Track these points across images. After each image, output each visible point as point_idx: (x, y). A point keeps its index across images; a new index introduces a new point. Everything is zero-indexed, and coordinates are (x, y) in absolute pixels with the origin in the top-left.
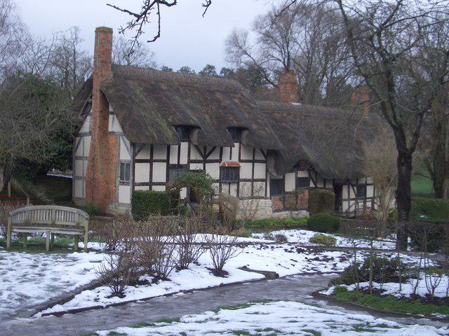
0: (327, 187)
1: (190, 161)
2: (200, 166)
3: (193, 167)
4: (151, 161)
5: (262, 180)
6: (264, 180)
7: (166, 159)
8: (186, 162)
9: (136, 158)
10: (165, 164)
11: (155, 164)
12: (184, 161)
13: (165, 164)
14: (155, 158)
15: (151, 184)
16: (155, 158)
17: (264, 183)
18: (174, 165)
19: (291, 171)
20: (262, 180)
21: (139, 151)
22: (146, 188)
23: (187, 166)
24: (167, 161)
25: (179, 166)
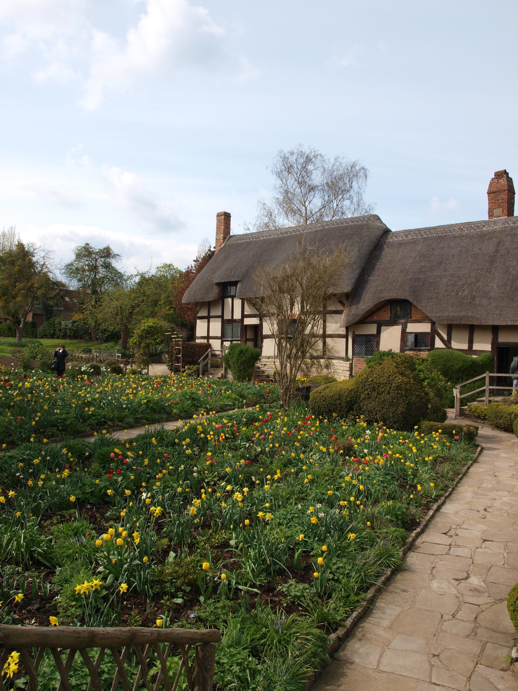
0: (476, 347)
1: (243, 316)
2: (254, 321)
3: (248, 321)
4: (208, 318)
5: (340, 336)
6: (346, 337)
7: (220, 314)
8: (240, 318)
9: (199, 315)
10: (220, 319)
11: (211, 319)
12: (237, 316)
13: (220, 319)
14: (211, 314)
15: (208, 337)
16: (211, 314)
17: (344, 340)
18: (228, 320)
19: (392, 323)
20: (340, 336)
21: (200, 309)
22: (205, 341)
23: (242, 320)
24: (222, 317)
25: (232, 321)
